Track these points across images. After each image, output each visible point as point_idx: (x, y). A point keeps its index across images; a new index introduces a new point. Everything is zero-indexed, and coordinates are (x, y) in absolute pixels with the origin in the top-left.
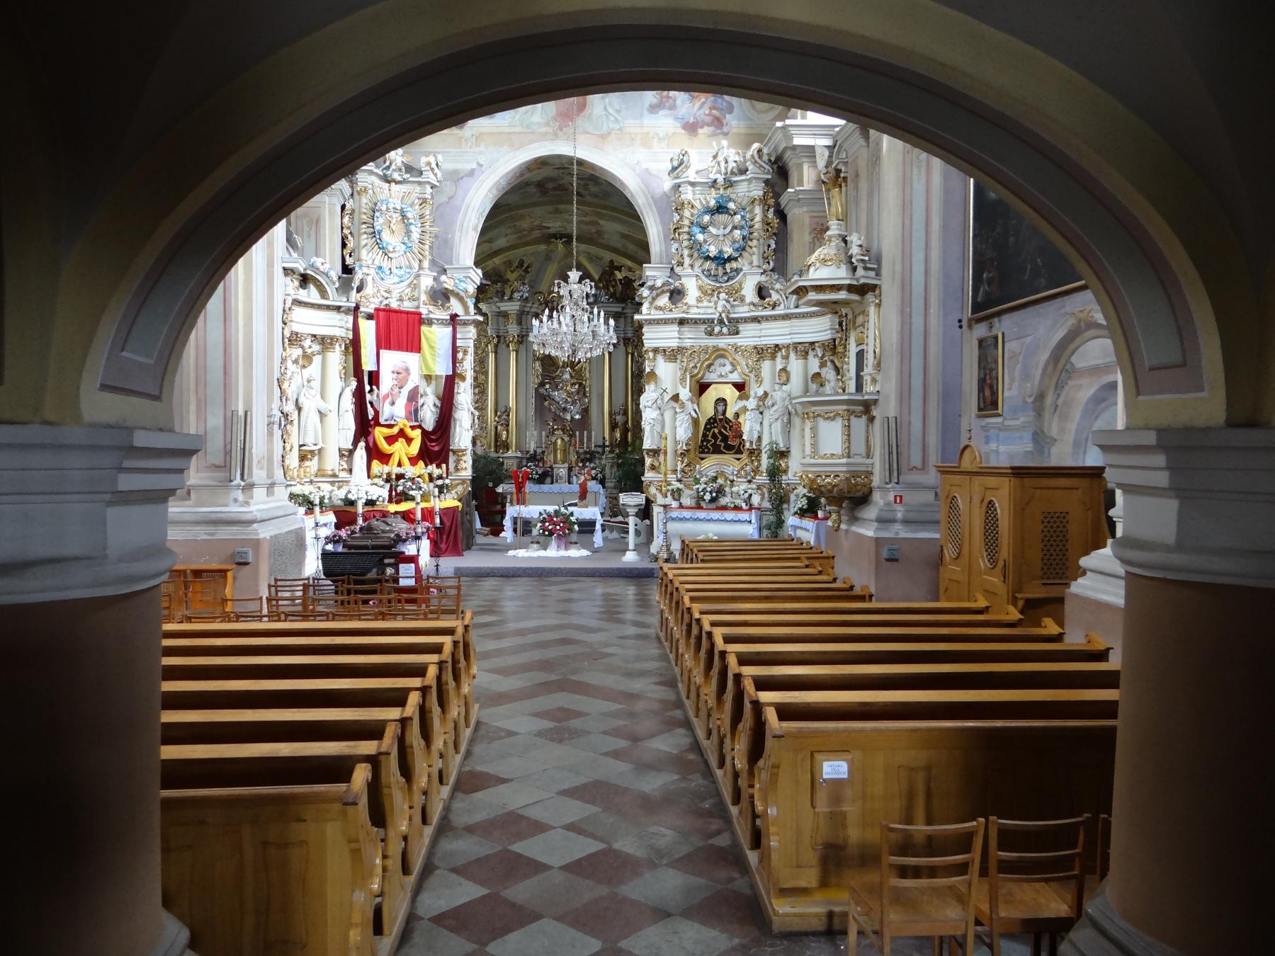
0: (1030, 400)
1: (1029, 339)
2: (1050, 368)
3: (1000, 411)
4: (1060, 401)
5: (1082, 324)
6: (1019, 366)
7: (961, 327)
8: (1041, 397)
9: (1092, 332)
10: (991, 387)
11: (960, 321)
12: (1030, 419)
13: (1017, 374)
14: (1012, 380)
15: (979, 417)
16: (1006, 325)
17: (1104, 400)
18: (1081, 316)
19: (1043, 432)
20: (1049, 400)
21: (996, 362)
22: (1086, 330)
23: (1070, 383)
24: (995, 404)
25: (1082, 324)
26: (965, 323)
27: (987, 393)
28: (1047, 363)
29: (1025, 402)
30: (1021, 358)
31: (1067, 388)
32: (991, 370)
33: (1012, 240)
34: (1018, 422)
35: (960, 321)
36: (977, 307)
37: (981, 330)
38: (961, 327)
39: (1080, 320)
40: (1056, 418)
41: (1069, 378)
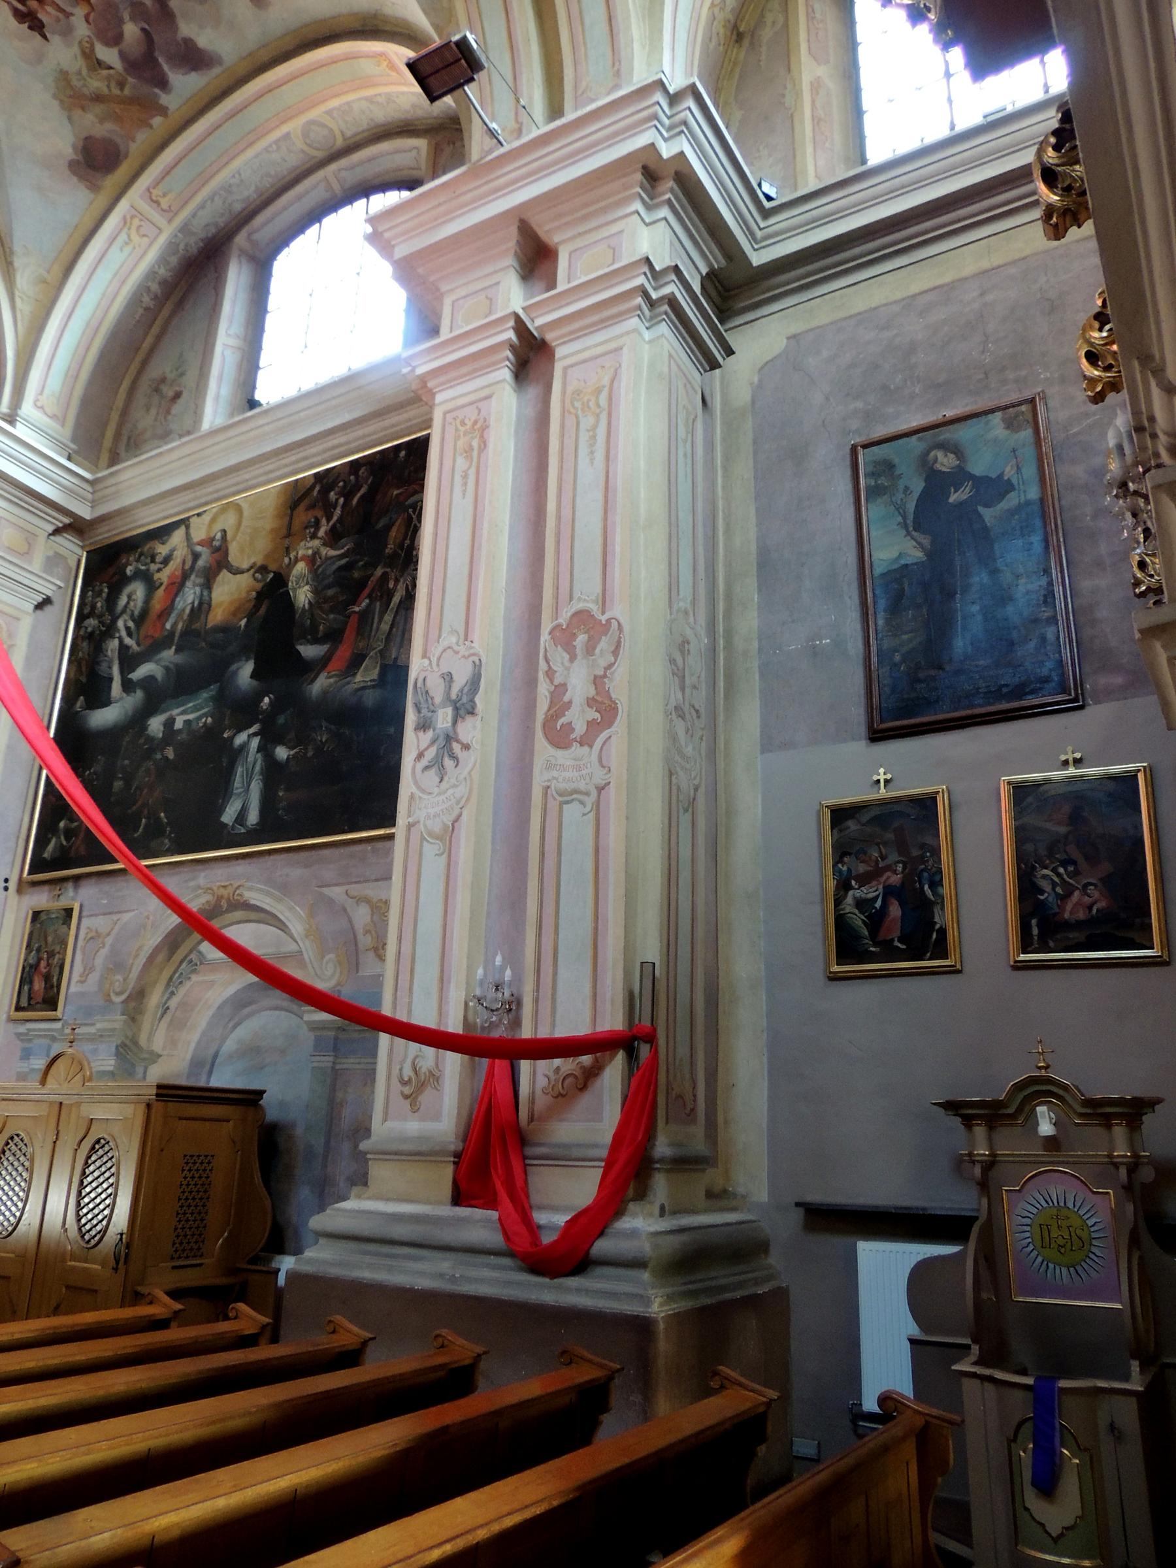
0: (118, 999)
1: (126, 917)
2: (161, 957)
3: (59, 1013)
4: (173, 1003)
5: (224, 904)
6: (104, 952)
7: (6, 889)
8: (139, 995)
9: (239, 914)
10: (47, 978)
11: (6, 881)
12: (117, 1025)
13: (99, 961)
14: (88, 969)
15: (11, 1020)
16: (84, 897)
17: (250, 1004)
18: (222, 891)
19: (136, 1043)
20: (154, 999)
21: (64, 943)
22: (228, 911)
23: (194, 978)
24: (51, 1003)
25: (224, 904)
26: (12, 885)
27: (38, 985)
28: (157, 950)
29: (108, 1000)
30: (109, 941)
31: (188, 984)
32: (51, 955)
33: (118, 785)
34: (92, 1030)
35: (6, 881)
36: (38, 865)
37: (41, 899)
38: (6, 889)
39: (220, 898)
40: (164, 1024)
41: (194, 971)
